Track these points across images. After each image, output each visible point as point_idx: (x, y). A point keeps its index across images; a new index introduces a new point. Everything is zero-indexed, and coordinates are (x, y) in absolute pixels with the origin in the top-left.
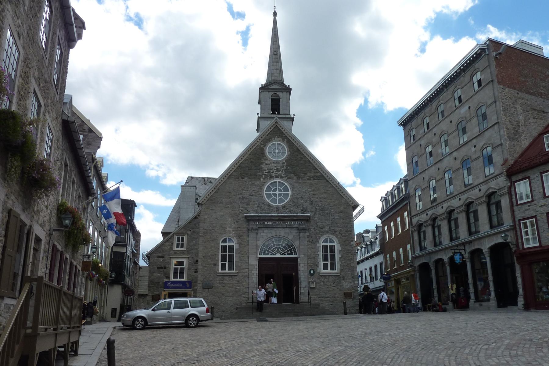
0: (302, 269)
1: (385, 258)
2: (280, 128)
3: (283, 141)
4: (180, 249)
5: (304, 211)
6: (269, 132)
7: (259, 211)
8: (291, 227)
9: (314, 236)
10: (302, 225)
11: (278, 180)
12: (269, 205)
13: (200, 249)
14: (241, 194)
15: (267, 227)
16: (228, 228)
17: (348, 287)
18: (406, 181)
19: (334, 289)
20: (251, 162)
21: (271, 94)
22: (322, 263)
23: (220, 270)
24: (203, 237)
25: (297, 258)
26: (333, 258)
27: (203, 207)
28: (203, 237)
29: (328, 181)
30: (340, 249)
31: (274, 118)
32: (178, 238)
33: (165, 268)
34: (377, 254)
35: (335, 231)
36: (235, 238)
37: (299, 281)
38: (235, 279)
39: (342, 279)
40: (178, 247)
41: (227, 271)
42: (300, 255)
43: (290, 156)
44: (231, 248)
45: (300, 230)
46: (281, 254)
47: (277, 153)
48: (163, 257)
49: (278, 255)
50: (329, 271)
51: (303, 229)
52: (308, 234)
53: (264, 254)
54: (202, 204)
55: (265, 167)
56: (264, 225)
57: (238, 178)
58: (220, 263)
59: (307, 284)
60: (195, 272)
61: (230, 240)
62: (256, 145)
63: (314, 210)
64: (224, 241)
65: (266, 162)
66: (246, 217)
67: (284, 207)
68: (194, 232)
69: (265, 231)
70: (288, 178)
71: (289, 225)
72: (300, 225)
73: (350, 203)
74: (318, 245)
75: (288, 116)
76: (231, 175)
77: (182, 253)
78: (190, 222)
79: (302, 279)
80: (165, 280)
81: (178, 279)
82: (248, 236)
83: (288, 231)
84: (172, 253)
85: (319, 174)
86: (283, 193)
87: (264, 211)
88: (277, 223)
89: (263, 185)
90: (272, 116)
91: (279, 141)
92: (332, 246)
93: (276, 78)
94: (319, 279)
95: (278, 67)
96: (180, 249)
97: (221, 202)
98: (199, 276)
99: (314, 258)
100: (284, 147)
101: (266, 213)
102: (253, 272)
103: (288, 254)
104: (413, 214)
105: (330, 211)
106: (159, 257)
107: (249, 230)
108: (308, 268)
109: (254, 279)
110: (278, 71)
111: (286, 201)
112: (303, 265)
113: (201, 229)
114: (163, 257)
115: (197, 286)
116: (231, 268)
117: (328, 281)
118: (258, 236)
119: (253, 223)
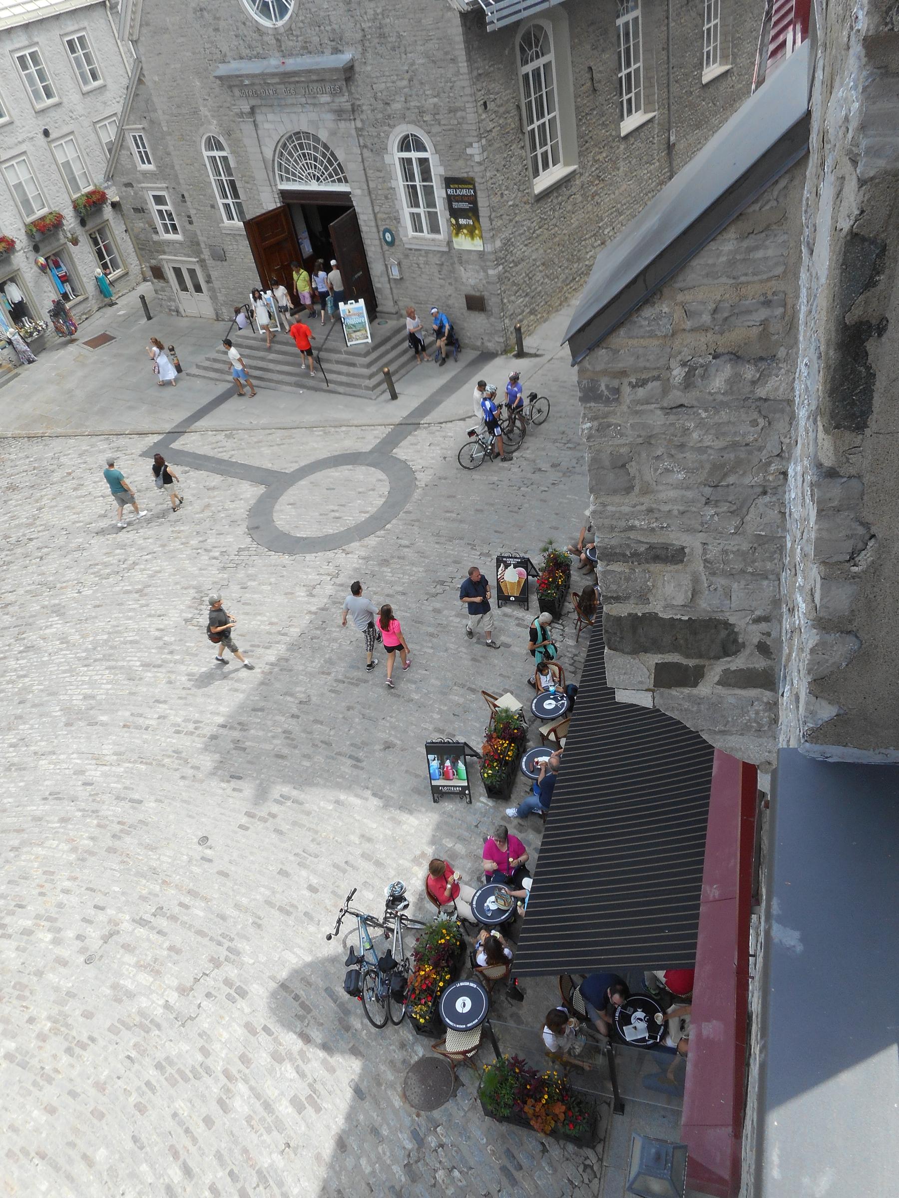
7: (245, 52)
9: (373, 131)
12: (258, 29)
13: (177, 167)
16: (201, 108)
17: (472, 282)
19: (442, 286)
22: (406, 211)
30: (441, 171)
32: (134, 137)
35: (421, 112)
39: (456, 260)
45: (340, 113)
48: (129, 185)
49: (314, 186)
50: (426, 234)
52: (359, 125)
59: (384, 268)
63: (359, 36)
67: (289, 30)
68: (152, 122)
69: (270, 117)
80: (155, 238)
83: (313, 116)
84: (139, 175)
94: (407, 256)
97: (166, 30)
98: (199, 233)
99: (386, 198)
105: (399, 36)
108: (377, 226)
113: (160, 112)
114: (129, 185)
115: (202, 253)
117: (426, 263)
118: (259, 132)
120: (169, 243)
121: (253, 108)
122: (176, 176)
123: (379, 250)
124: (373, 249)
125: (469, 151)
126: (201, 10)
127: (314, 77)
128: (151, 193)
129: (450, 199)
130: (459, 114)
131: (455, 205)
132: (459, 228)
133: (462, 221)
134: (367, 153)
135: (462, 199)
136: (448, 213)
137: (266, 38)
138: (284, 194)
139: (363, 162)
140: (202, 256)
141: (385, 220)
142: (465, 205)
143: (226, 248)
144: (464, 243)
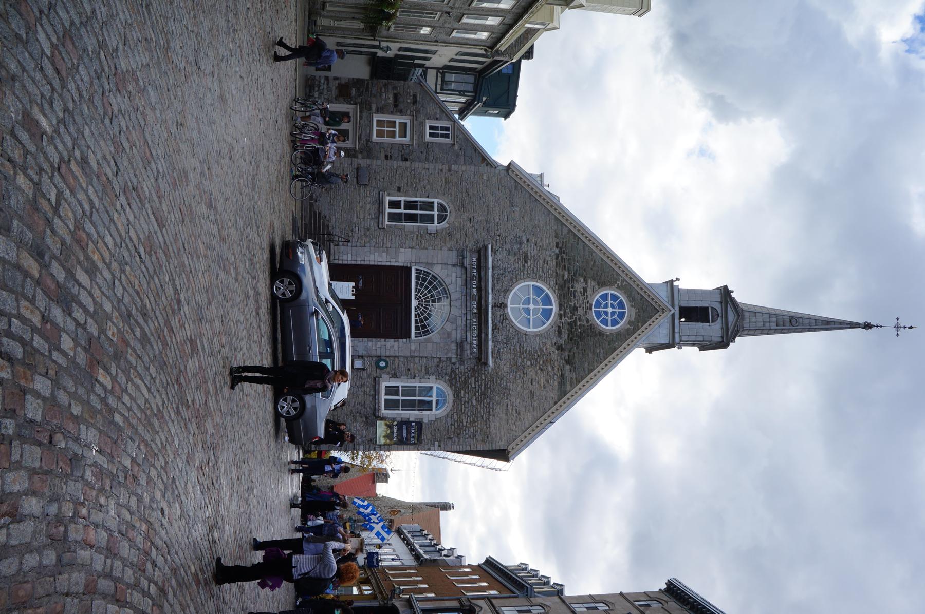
0: (388, 344)
1: (410, 568)
2: (653, 319)
3: (630, 323)
4: (428, 131)
5: (497, 354)
6: (646, 297)
7: (497, 272)
8: (467, 327)
10: (471, 348)
11: (555, 307)
12: (507, 291)
14: (528, 241)
15: (466, 284)
18: (558, 591)
20: (587, 261)
21: (718, 307)
23: (388, 198)
24: (450, 170)
25: (409, 336)
26: (409, 405)
27: (503, 173)
28: (450, 170)
29: (556, 403)
30: (426, 420)
31: (673, 306)
32: (447, 129)
33: (396, 106)
34: (417, 557)
36: (447, 225)
37: (365, 340)
38: (373, 224)
40: (431, 128)
41: (388, 210)
42: (415, 342)
43: (601, 334)
44: (430, 219)
45: (460, 345)
46: (417, 308)
47: (604, 309)
48: (415, 102)
49: (414, 303)
51: (463, 350)
52: (453, 360)
53: (417, 278)
54: (507, 171)
55: (579, 287)
56: (471, 279)
57: (556, 237)
58: (403, 199)
60: (387, 157)
61: (442, 218)
62: (620, 273)
64: (442, 208)
65: (589, 291)
66: (486, 248)
67: (505, 317)
68: (458, 156)
69: (459, 280)
70: (559, 327)
71: (471, 325)
72: (471, 344)
73: (514, 444)
74: (433, 378)
75: (677, 336)
76: (563, 224)
77: (422, 135)
78: (476, 150)
79: (370, 344)
80: (374, 108)
81: (375, 128)
82: (451, 249)
85: (568, 387)
86: (532, 317)
87: (497, 280)
88: (475, 303)
89: (544, 281)
90: (677, 308)
91: (630, 316)
92: (431, 407)
93: (747, 320)
94: (369, 376)
95: (767, 325)
96: (428, 131)
98: (379, 162)
100: (618, 323)
101: (493, 285)
102: (384, 254)
103: (416, 321)
104: (494, 601)
106: (415, 96)
107: (462, 251)
108: (389, 357)
109: (372, 257)
110: (761, 324)
111: (516, 323)
112: (396, 348)
113: (464, 168)
114: (415, 102)
116: (392, 217)
119: (474, 259)
120: (371, 121)
121: (466, 269)
122: (420, 161)
123: (374, 353)
124: (374, 348)
125: (436, 443)
126: (520, 243)
127: (483, 335)
128: (408, 122)
129: (407, 423)
130: (457, 439)
131: (405, 427)
132: (390, 427)
133: (395, 430)
134: (436, 361)
135: (409, 433)
136: (399, 419)
137: (502, 294)
138: (409, 270)
139: (432, 357)
140: (360, 156)
141: (394, 364)
142: (405, 435)
143: (368, 188)
144: (381, 429)
